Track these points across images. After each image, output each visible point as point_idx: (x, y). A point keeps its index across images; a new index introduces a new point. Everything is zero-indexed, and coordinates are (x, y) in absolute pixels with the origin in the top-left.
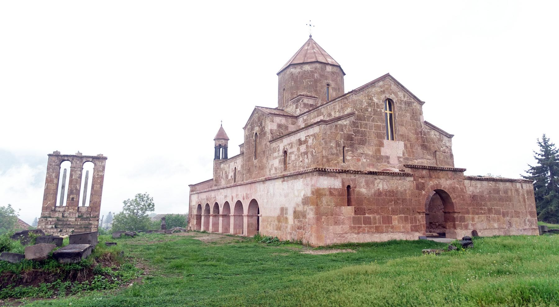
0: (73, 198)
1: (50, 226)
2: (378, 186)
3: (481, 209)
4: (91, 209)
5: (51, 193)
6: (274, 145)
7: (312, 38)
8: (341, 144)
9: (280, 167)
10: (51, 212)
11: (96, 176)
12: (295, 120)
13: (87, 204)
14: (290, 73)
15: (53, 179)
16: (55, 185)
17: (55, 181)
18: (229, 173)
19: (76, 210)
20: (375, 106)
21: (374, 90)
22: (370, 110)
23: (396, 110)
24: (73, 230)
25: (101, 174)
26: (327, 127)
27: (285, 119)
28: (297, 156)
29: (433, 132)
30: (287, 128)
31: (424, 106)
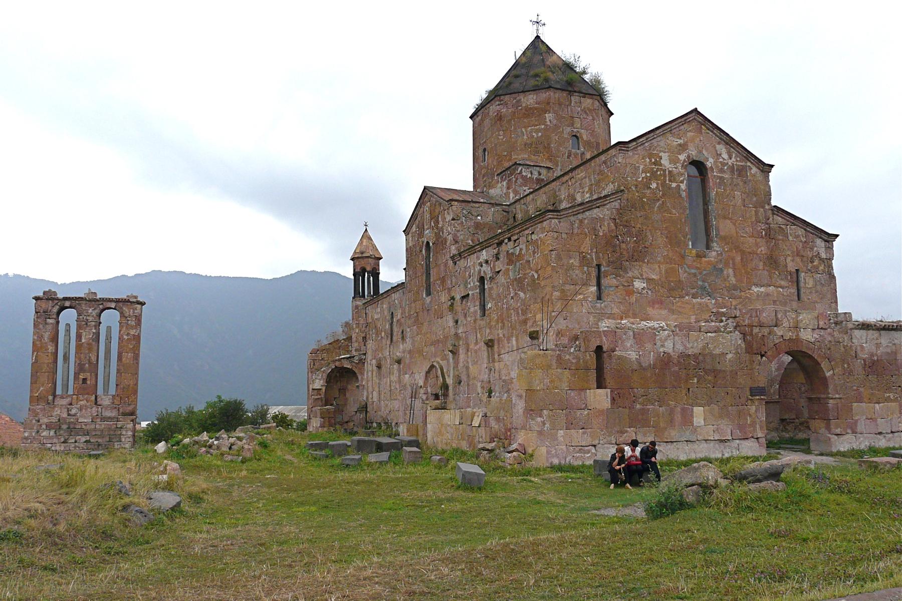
0: (85, 380)
2: (663, 346)
3: (889, 389)
5: (44, 371)
8: (592, 259)
11: (125, 337)
13: (112, 390)
16: (50, 354)
17: (51, 348)
19: (92, 401)
20: (665, 176)
21: (662, 144)
22: (654, 186)
23: (711, 184)
26: (561, 224)
29: (791, 229)
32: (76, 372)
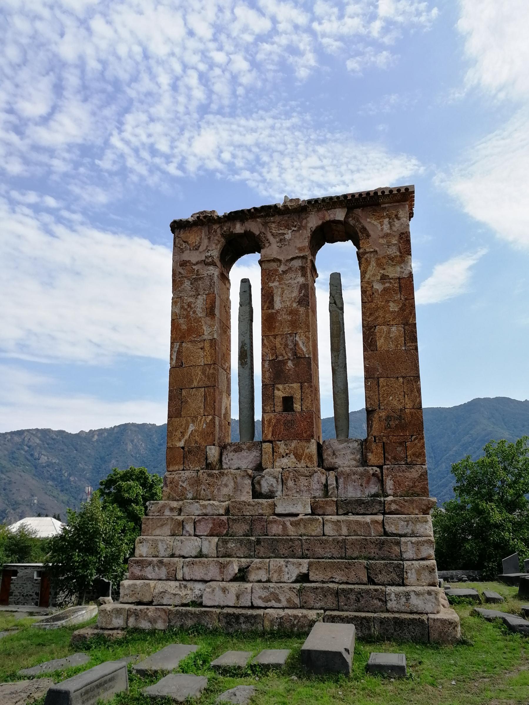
4: (380, 450)
5: (195, 384)
10: (203, 475)
11: (378, 287)
15: (198, 320)
16: (207, 345)
19: (310, 457)
24: (304, 570)
25: (393, 272)
32: (267, 382)
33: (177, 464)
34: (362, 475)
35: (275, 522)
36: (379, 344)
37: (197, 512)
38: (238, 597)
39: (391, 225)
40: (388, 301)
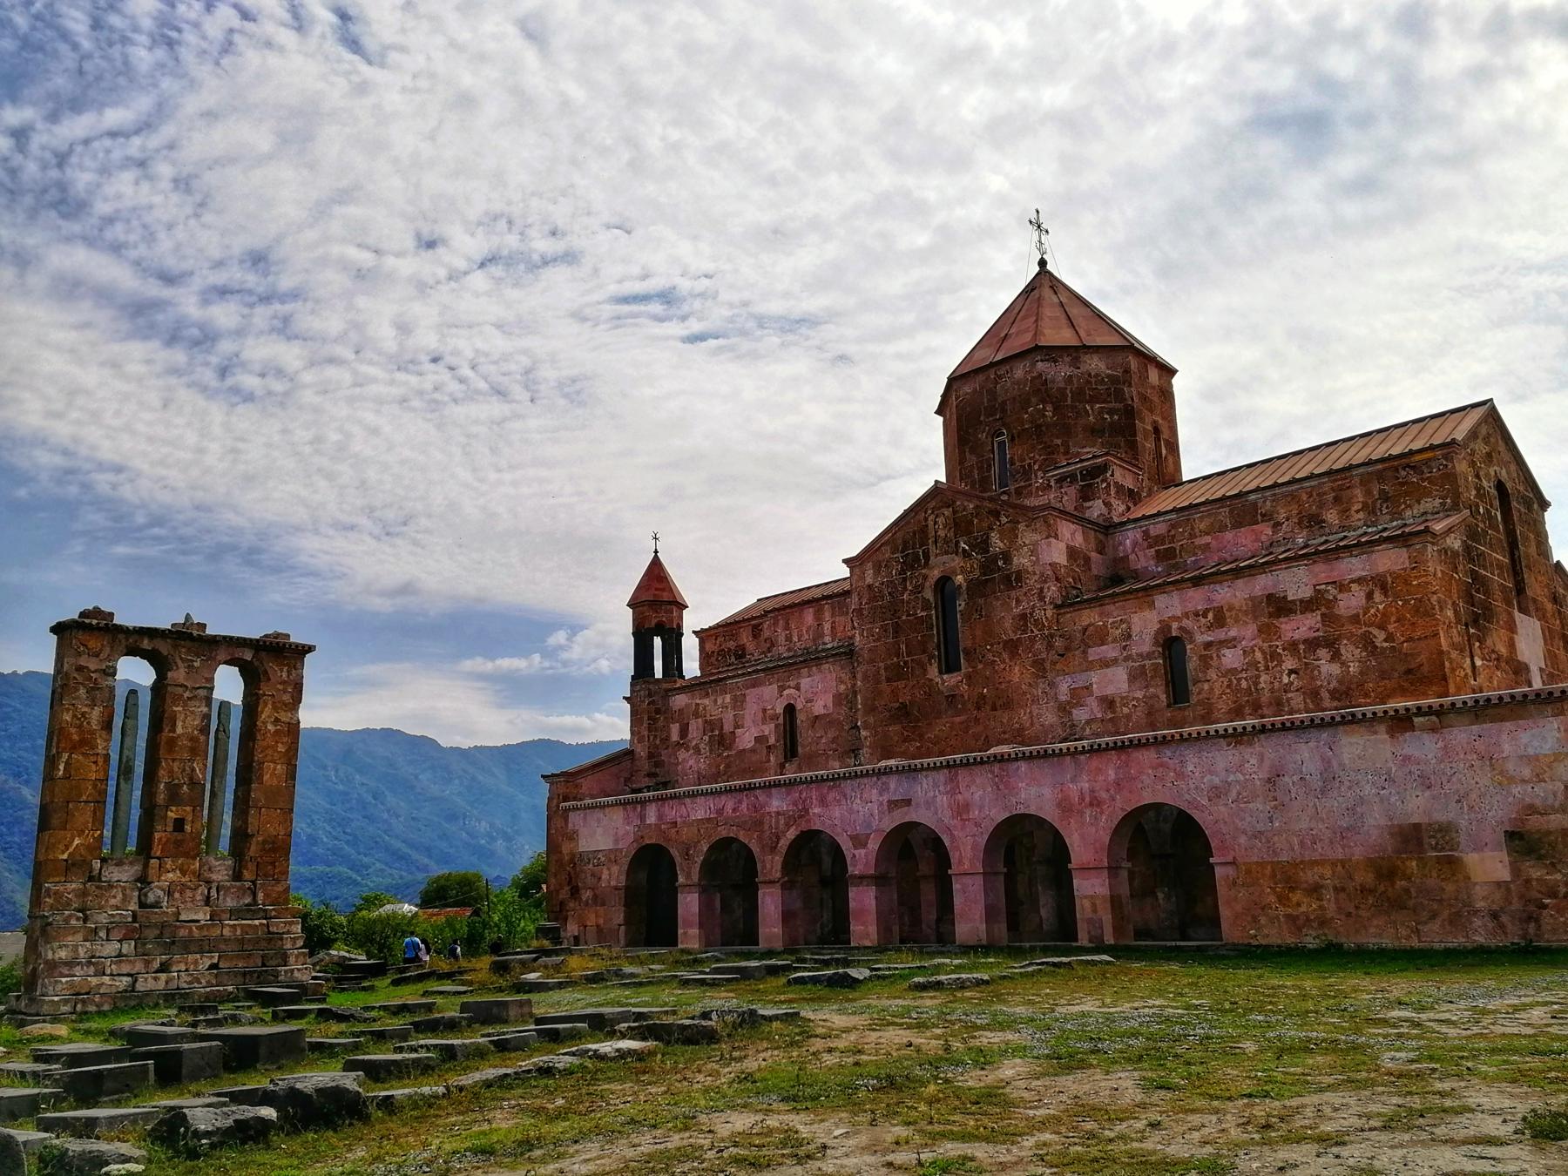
0: (179, 824)
1: (111, 948)
4: (255, 868)
5: (84, 798)
6: (1089, 617)
7: (1049, 267)
9: (1139, 694)
11: (270, 727)
12: (1101, 537)
14: (1033, 379)
15: (93, 733)
16: (100, 760)
18: (737, 727)
19: (194, 873)
22: (1481, 511)
24: (215, 961)
25: (285, 717)
27: (1083, 532)
28: (1258, 655)
30: (1087, 560)
31: (1548, 515)
33: (58, 875)
34: (239, 888)
35: (183, 927)
36: (265, 778)
37: (105, 921)
38: (167, 983)
39: (289, 672)
40: (277, 742)
